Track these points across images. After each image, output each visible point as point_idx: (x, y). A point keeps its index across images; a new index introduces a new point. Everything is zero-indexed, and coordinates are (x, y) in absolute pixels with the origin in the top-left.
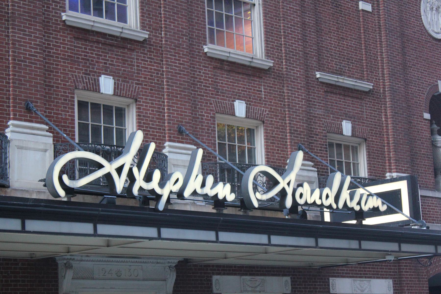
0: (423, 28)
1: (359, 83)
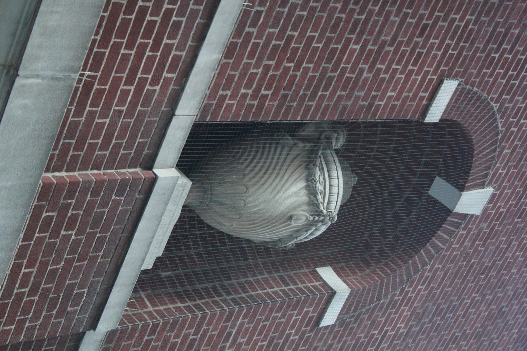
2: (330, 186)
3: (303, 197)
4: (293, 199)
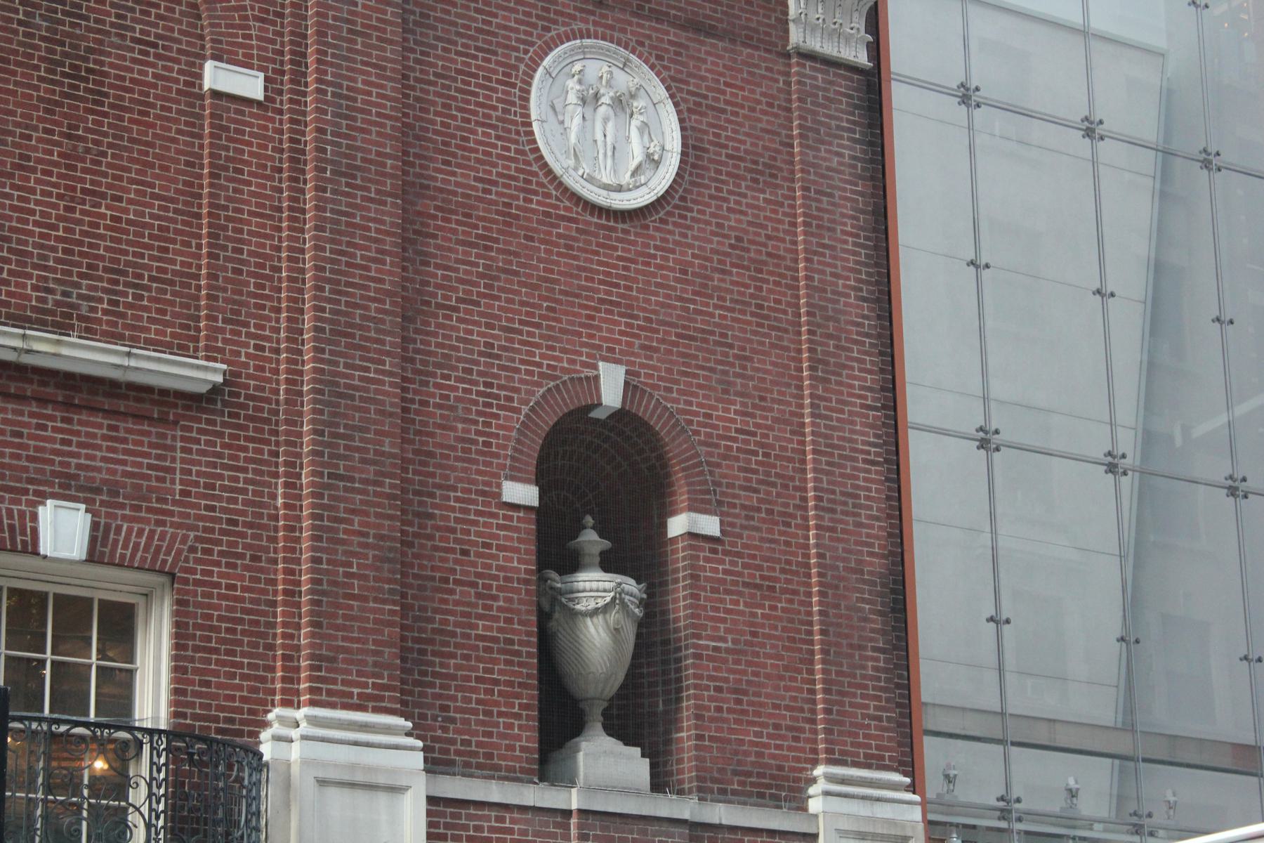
0: (535, 168)
1: (149, 358)
2: (591, 591)
3: (599, 619)
4: (601, 630)
